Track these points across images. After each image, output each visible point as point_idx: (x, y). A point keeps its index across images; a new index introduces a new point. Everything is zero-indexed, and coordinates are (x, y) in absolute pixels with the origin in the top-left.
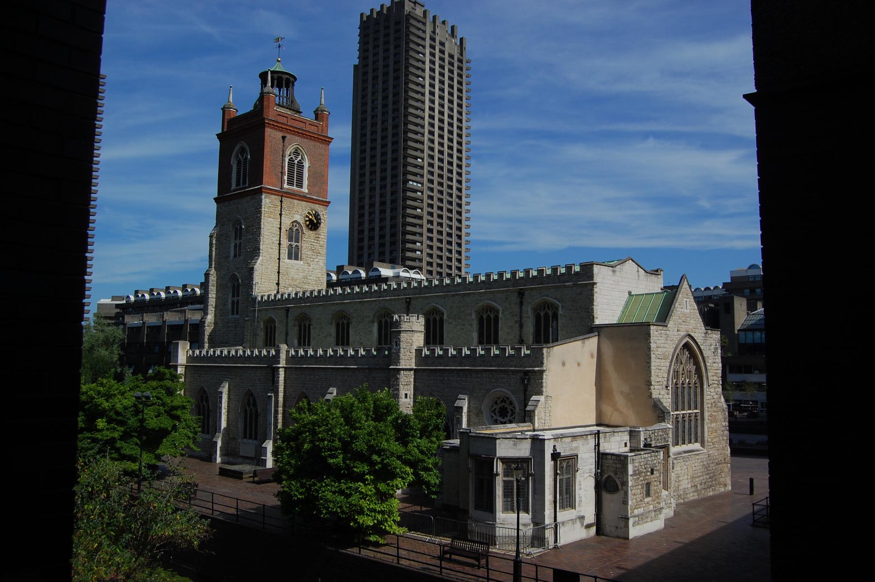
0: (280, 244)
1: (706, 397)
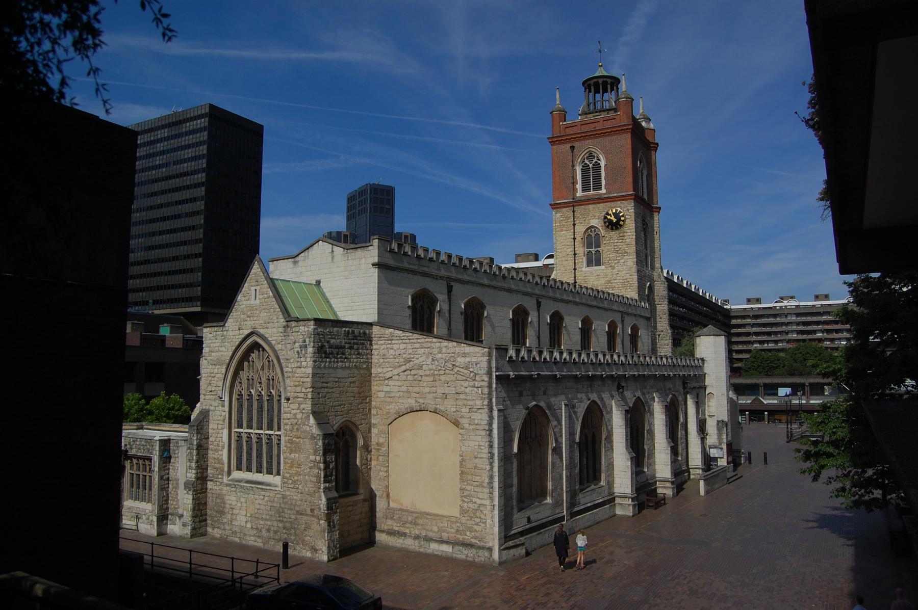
0: (575, 254)
1: (283, 416)
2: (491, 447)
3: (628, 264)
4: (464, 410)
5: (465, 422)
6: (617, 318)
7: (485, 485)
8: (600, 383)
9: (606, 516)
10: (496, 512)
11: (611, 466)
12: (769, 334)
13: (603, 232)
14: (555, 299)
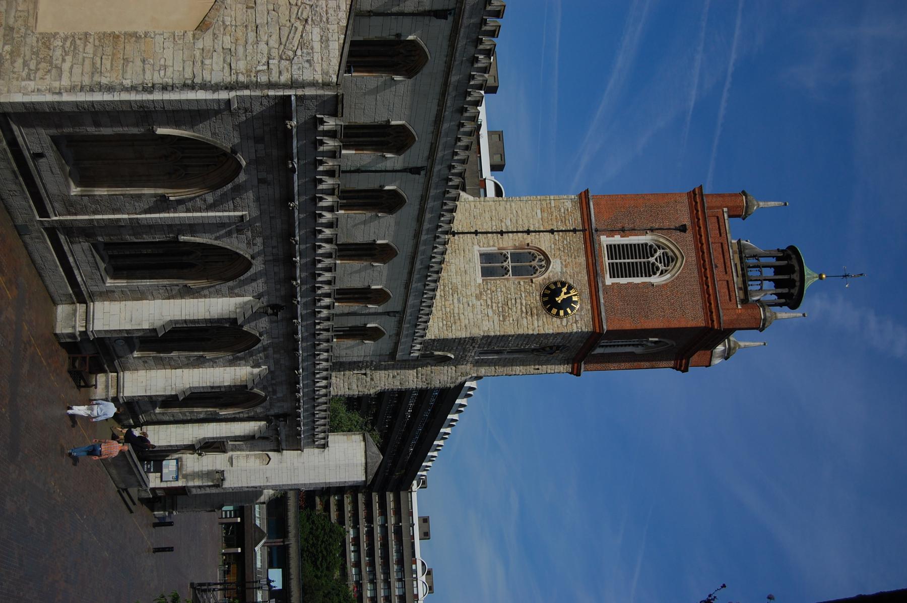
0: (502, 233)
2: (165, 88)
3: (486, 323)
4: (227, 39)
5: (206, 40)
6: (394, 304)
7: (97, 78)
8: (282, 275)
9: (52, 289)
10: (49, 98)
11: (139, 295)
12: (371, 553)
13: (539, 279)
14: (424, 199)
